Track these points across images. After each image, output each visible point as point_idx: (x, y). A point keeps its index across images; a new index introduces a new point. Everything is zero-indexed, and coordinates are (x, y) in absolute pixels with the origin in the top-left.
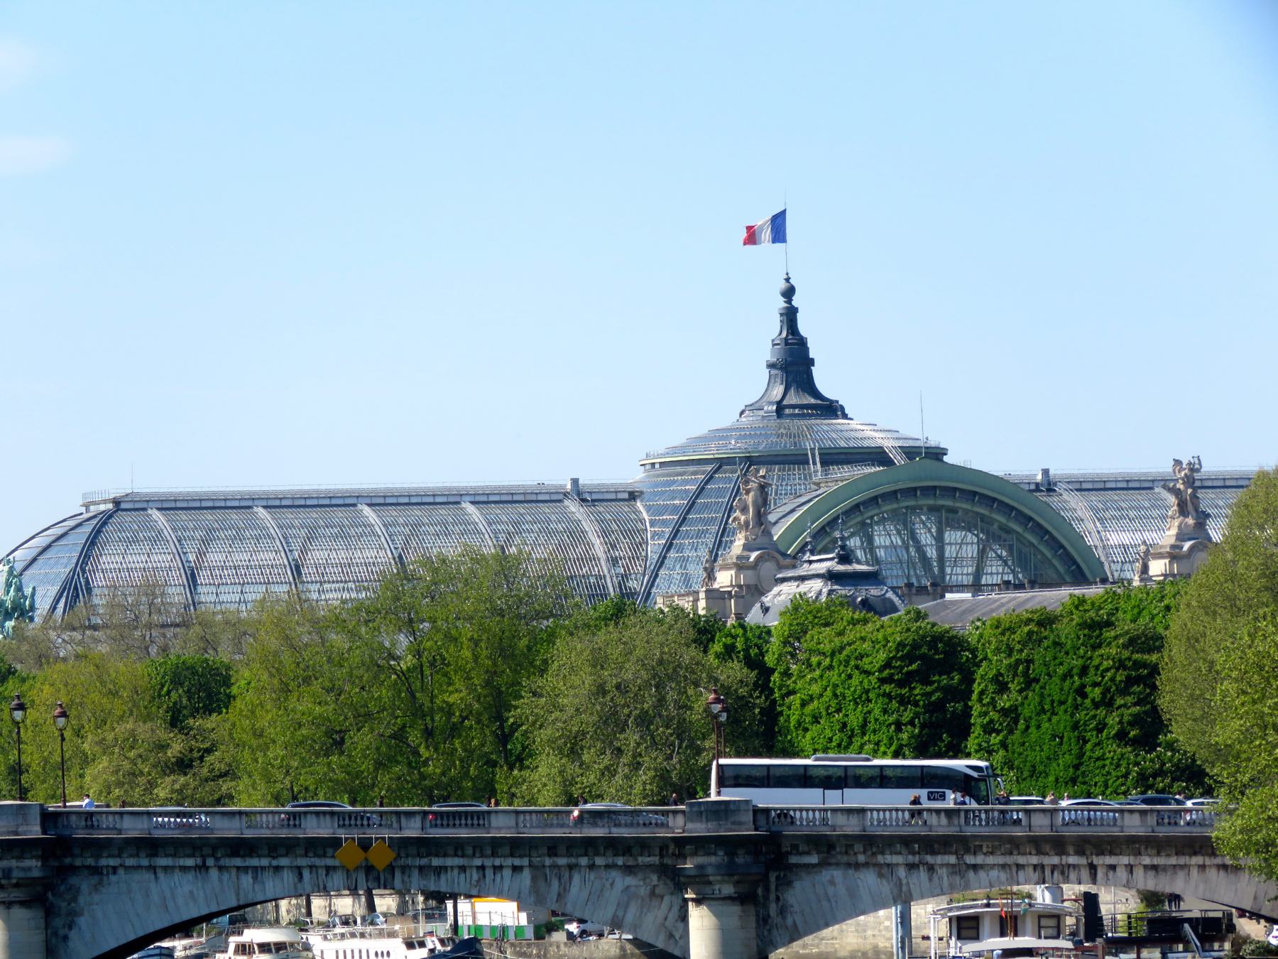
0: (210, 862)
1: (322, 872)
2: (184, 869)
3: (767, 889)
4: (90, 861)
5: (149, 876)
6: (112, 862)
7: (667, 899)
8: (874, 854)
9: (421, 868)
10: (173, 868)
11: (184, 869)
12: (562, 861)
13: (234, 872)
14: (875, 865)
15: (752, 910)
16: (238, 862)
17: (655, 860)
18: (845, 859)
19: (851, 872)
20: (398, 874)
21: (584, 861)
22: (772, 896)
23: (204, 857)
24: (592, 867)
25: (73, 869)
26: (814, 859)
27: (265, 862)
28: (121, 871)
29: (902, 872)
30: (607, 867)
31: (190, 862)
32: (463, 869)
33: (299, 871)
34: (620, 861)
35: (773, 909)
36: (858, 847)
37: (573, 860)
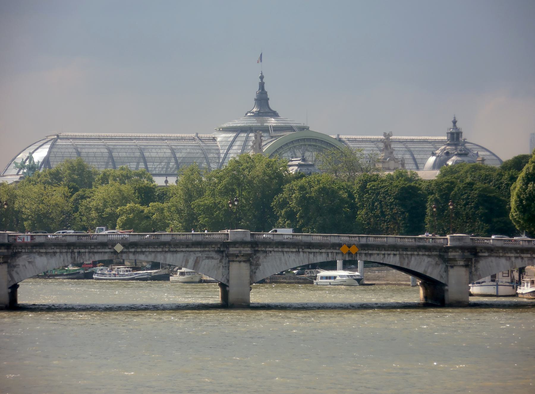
0: (301, 250)
1: (335, 254)
2: (292, 252)
3: (472, 263)
4: (264, 249)
5: (281, 254)
6: (270, 249)
7: (441, 265)
8: (505, 253)
9: (365, 254)
10: (289, 252)
11: (292, 252)
12: (409, 253)
13: (308, 253)
14: (506, 257)
15: (468, 269)
16: (309, 250)
17: (437, 253)
18: (496, 255)
19: (498, 258)
20: (358, 255)
21: (416, 253)
22: (473, 265)
23: (299, 249)
24: (418, 255)
25: (258, 251)
26: (486, 254)
27: (317, 250)
28: (273, 252)
29: (513, 259)
30: (423, 255)
31: (294, 250)
32: (378, 254)
33: (328, 254)
34: (427, 253)
35: (473, 269)
36: (501, 251)
37: (412, 253)
